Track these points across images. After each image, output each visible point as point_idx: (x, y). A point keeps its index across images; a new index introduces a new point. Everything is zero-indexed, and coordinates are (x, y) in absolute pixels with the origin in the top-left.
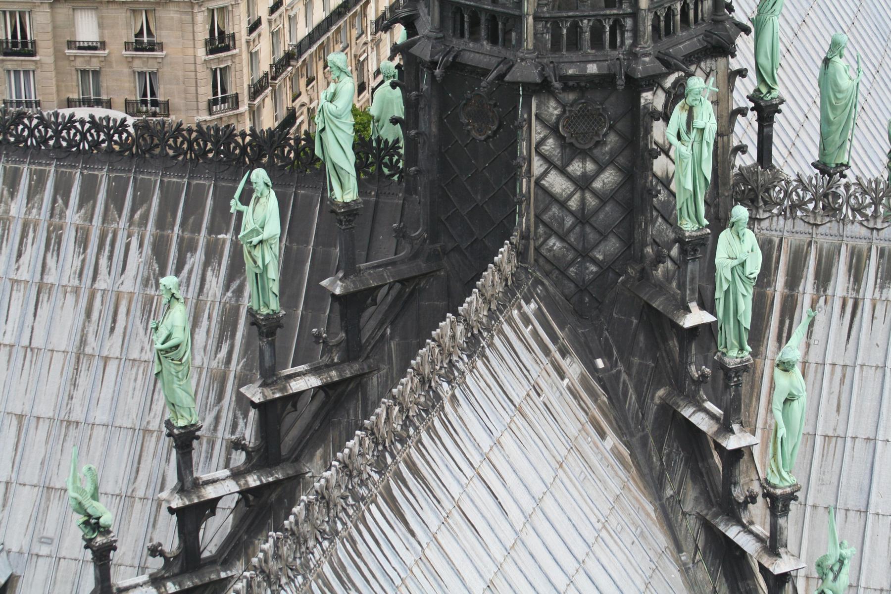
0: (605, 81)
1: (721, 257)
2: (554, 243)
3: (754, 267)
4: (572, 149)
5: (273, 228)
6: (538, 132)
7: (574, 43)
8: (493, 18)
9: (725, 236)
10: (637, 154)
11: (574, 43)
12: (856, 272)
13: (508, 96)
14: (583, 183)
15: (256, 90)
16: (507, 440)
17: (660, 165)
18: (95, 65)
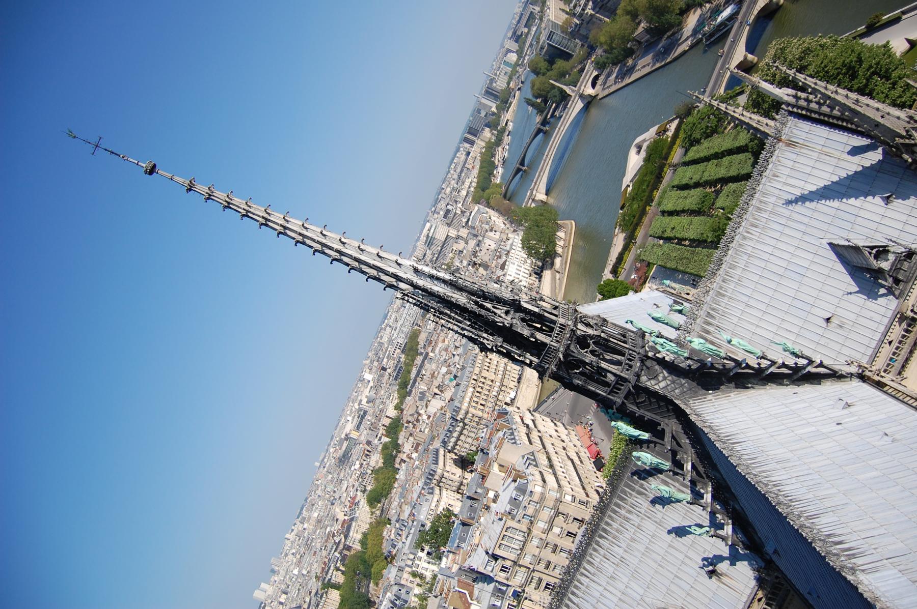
0: (642, 361)
1: (697, 347)
2: (677, 391)
3: (702, 341)
4: (655, 377)
5: (649, 456)
6: (648, 383)
7: (631, 366)
8: (617, 383)
9: (693, 345)
10: (662, 362)
11: (631, 366)
12: (709, 324)
13: (636, 387)
14: (665, 378)
15: (587, 496)
16: (725, 415)
17: (667, 359)
18: (566, 532)
